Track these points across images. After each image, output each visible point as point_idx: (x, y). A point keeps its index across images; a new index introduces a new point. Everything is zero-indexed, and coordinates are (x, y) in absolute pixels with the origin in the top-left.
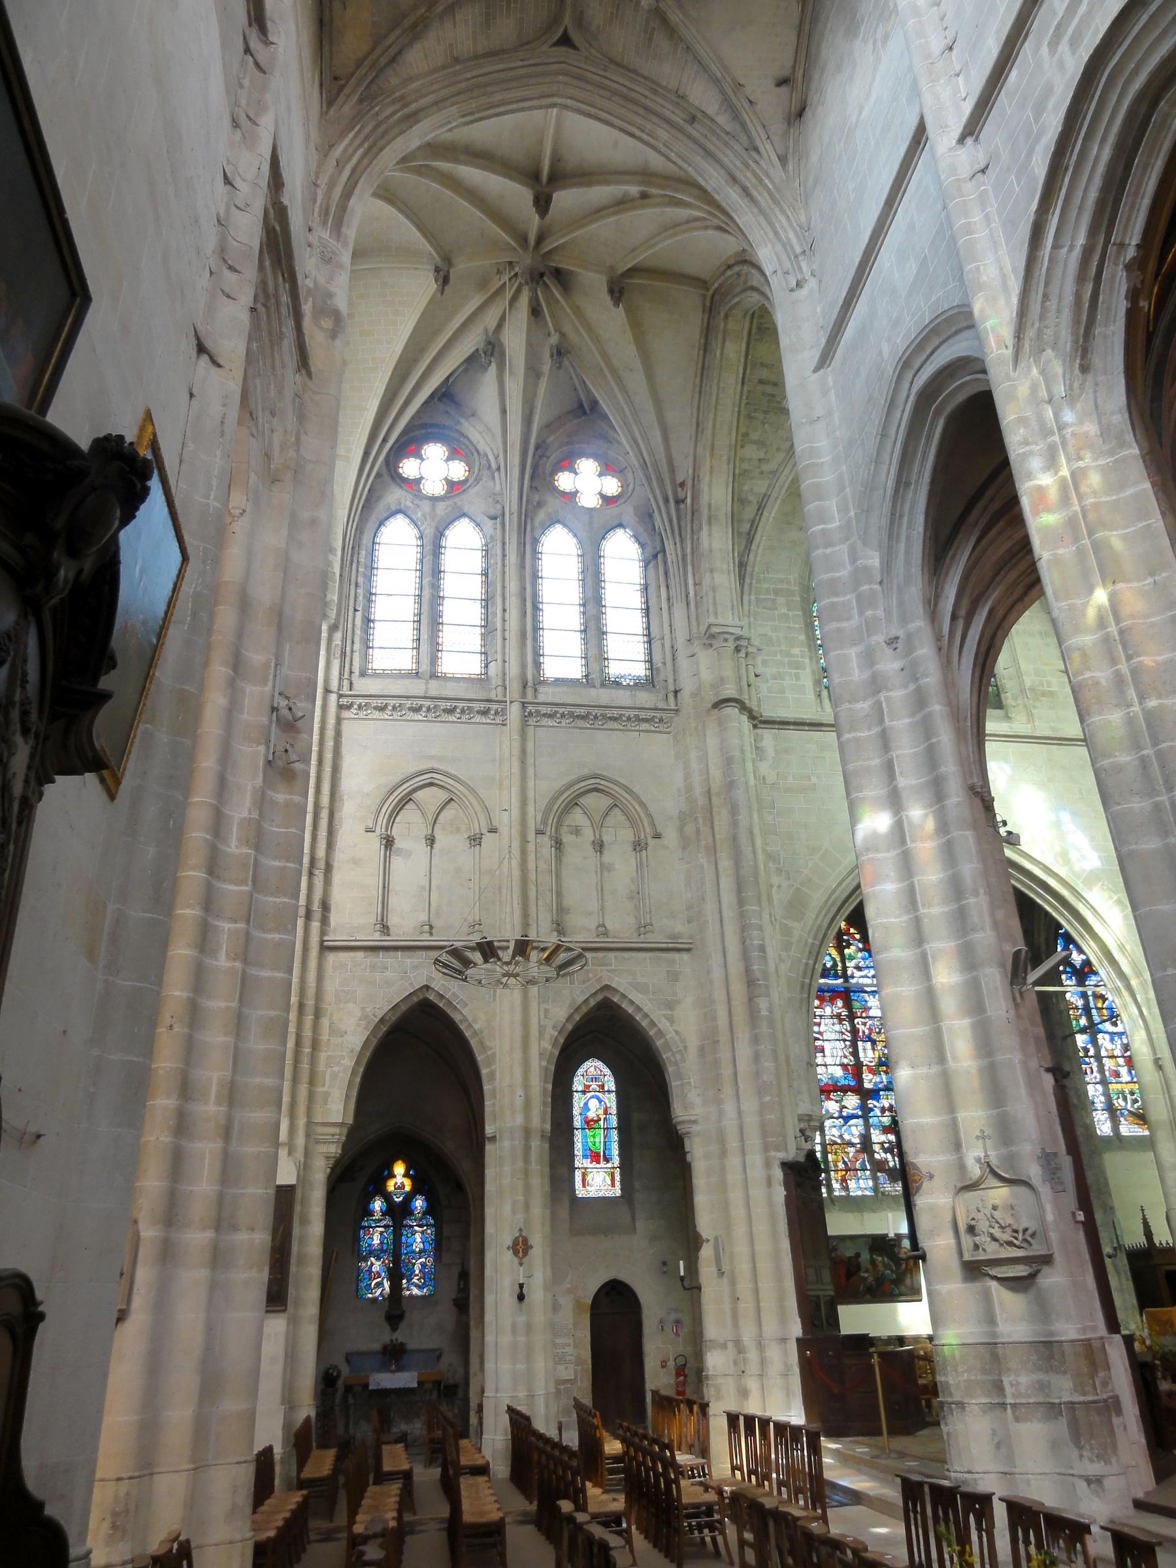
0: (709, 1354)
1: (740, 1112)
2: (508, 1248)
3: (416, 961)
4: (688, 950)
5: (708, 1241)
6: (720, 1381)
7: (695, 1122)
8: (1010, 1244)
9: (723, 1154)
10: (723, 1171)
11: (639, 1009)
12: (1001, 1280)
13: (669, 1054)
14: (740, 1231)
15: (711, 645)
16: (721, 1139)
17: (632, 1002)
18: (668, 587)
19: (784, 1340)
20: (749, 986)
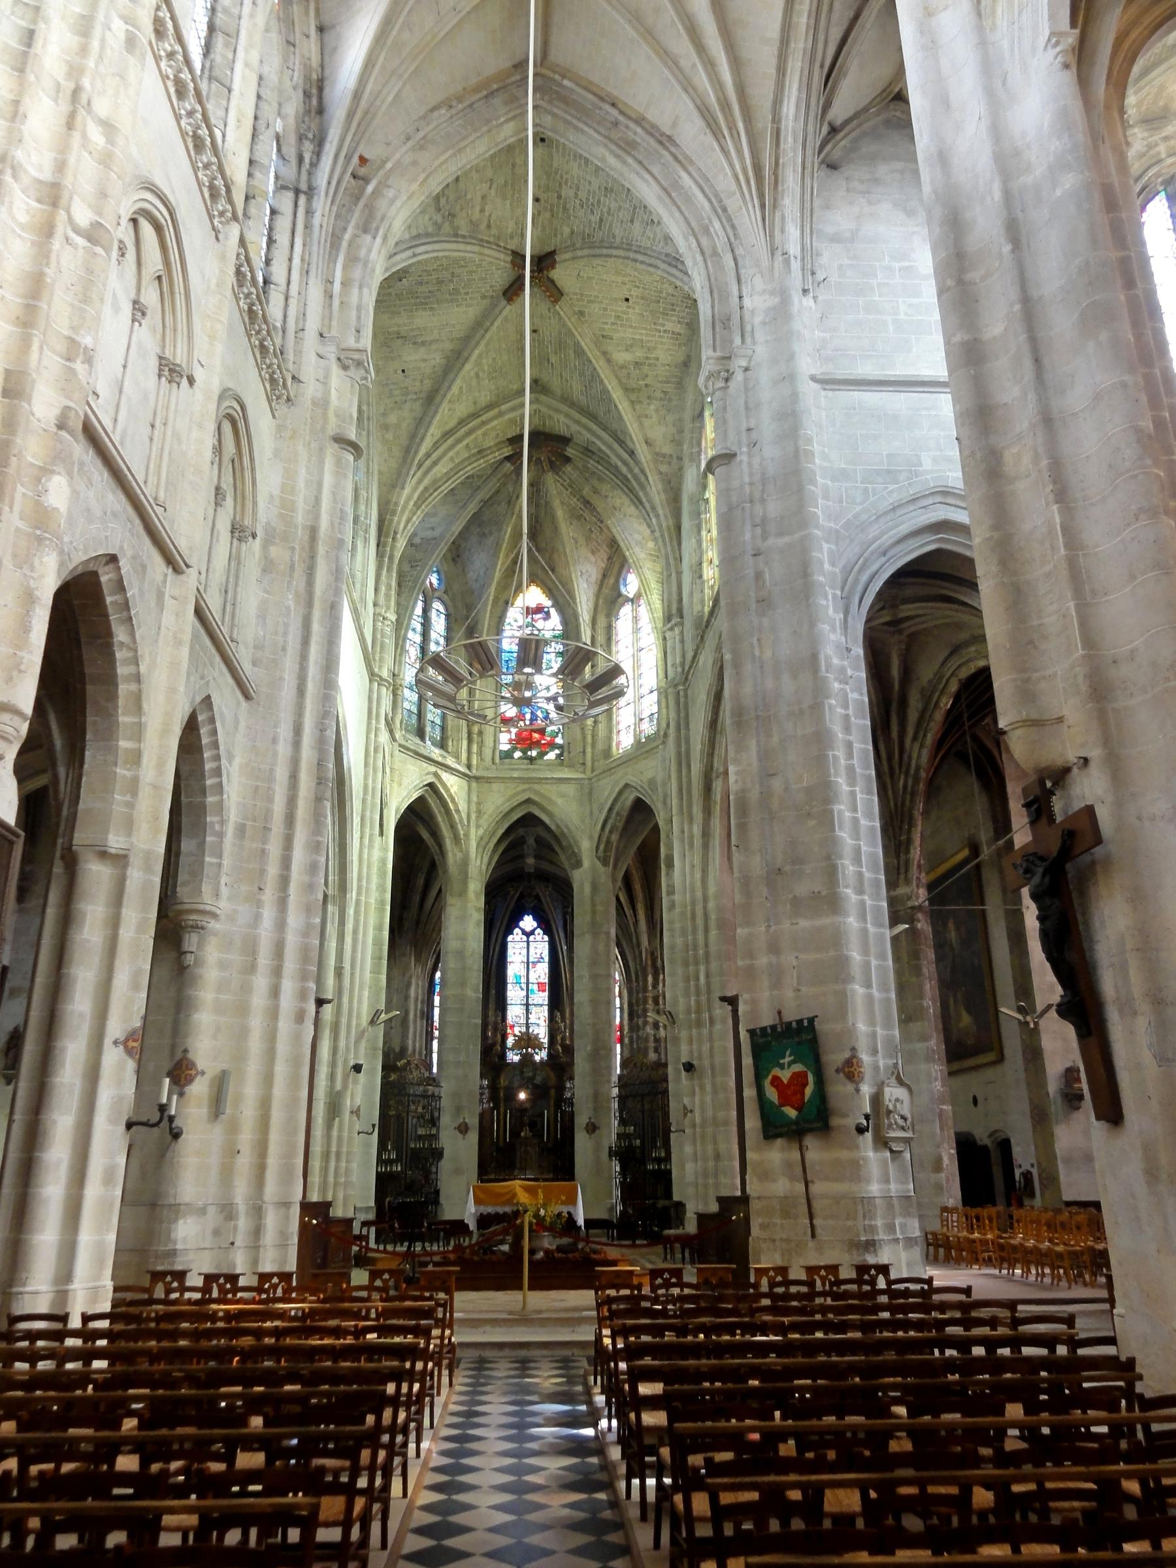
0: (181, 1222)
1: (281, 925)
2: (116, 1043)
3: (118, 507)
4: (247, 697)
5: (203, 1073)
6: (191, 1256)
7: (214, 916)
8: (903, 1128)
9: (251, 968)
10: (246, 989)
11: (215, 745)
12: (892, 1151)
13: (215, 819)
14: (253, 1067)
15: (345, 368)
16: (250, 948)
17: (214, 732)
18: (304, 245)
19: (287, 1205)
20: (319, 784)
